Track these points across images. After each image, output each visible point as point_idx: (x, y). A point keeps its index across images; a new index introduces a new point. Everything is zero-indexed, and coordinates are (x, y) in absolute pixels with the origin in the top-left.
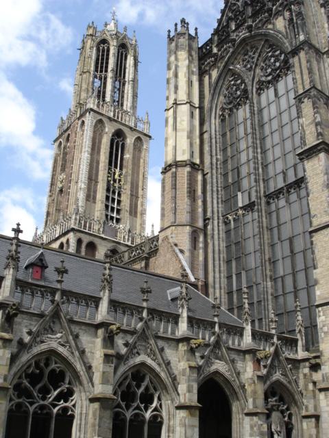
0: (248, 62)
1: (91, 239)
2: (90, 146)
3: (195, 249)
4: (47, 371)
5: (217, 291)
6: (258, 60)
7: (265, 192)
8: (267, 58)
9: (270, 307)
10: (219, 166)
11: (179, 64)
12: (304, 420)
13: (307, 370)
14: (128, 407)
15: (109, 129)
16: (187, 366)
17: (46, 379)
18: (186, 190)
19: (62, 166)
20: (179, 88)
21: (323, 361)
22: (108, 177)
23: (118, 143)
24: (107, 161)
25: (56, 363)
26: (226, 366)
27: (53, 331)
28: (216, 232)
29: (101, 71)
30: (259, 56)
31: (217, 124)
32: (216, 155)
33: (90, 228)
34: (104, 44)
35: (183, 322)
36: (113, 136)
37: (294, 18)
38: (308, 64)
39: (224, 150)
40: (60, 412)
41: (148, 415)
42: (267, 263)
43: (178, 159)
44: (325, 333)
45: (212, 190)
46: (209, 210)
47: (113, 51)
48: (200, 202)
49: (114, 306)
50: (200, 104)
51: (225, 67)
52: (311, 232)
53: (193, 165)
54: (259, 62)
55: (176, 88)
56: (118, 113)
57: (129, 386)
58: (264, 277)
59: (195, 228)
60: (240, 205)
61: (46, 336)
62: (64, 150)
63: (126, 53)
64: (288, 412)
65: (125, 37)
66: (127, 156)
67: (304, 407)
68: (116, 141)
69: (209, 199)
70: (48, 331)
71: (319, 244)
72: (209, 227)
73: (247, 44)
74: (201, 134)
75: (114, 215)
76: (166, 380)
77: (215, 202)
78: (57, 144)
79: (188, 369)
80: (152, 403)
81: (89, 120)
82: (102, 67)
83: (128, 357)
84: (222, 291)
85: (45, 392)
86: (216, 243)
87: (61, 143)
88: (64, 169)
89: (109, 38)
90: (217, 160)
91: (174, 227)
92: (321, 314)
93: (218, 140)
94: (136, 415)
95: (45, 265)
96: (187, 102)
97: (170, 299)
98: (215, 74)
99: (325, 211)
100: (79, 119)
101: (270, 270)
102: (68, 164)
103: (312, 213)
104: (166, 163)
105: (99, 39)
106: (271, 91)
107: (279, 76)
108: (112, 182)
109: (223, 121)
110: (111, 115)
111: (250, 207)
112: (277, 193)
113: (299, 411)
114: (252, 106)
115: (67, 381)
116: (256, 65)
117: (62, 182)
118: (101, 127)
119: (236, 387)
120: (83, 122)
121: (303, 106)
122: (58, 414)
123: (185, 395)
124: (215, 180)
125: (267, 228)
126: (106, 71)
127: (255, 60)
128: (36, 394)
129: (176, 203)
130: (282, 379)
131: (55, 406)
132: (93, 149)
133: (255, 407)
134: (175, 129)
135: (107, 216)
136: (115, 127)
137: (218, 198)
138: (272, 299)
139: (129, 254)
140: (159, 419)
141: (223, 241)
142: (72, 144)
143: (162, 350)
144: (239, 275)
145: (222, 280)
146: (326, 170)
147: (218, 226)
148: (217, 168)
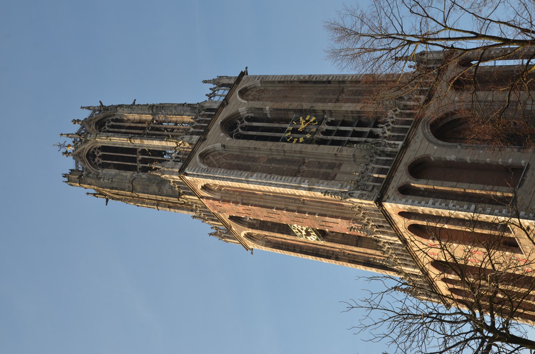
2: (239, 173)
22: (298, 142)
23: (243, 128)
24: (270, 144)
29: (134, 160)
34: (95, 156)
36: (231, 137)
47: (103, 140)
63: (113, 120)
65: (85, 123)
68: (240, 131)
89: (87, 147)
108: (308, 136)
118: (213, 156)
126: (133, 151)
132: (246, 169)
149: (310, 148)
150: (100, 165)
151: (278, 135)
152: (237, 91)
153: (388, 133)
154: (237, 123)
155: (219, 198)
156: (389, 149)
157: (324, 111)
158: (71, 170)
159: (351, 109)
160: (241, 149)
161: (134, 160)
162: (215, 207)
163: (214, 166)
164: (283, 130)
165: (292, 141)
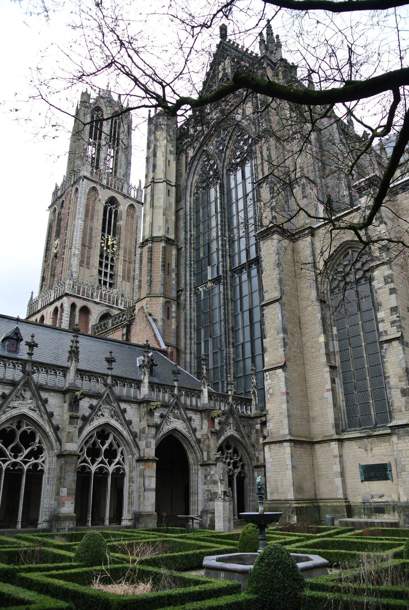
0: (221, 144)
1: (85, 303)
2: (84, 213)
3: (168, 318)
4: (19, 433)
5: (188, 356)
6: (228, 143)
7: (230, 267)
8: (238, 141)
9: (232, 370)
10: (192, 242)
11: (158, 144)
12: (255, 469)
13: (258, 427)
14: (93, 462)
15: (104, 195)
16: (146, 425)
17: (18, 440)
18: (160, 264)
19: (56, 232)
20: (157, 167)
21: (268, 419)
22: (102, 243)
24: (101, 228)
25: (27, 426)
26: (184, 424)
27: (24, 398)
28: (188, 303)
30: (230, 139)
31: (192, 201)
32: (190, 231)
33: (84, 292)
35: (144, 387)
36: (106, 203)
37: (259, 106)
38: (268, 152)
39: (197, 226)
40: (31, 467)
41: (111, 469)
42: (231, 332)
43: (155, 235)
44: (271, 394)
45: (186, 264)
46: (183, 282)
48: (173, 275)
49: (80, 375)
50: (176, 182)
51: (199, 148)
52: (263, 306)
53: (168, 241)
54: (230, 145)
55: (154, 167)
56: (112, 180)
57: (94, 443)
58: (227, 344)
59: (168, 300)
60: (209, 278)
61: (18, 402)
62: (58, 217)
64: (241, 463)
66: (121, 223)
67: (255, 459)
68: (109, 208)
69: (182, 273)
70: (19, 398)
71: (269, 317)
72: (182, 298)
73: (220, 127)
74: (177, 211)
75: (108, 280)
76: (128, 437)
77: (188, 275)
78: (52, 210)
79: (147, 429)
80: (115, 457)
81: (84, 186)
82: (96, 135)
83: (93, 419)
84: (193, 356)
85: (16, 451)
86: (188, 312)
87: (55, 210)
88: (59, 235)
90: (191, 236)
91: (149, 298)
92: (268, 378)
93: (192, 217)
94: (101, 469)
95: (20, 338)
96: (164, 181)
97: (138, 366)
98: (191, 153)
99: (275, 288)
100: (72, 186)
101: (233, 338)
102: (62, 231)
103: (265, 289)
104: (144, 237)
105: (93, 106)
106: (239, 174)
107: (246, 159)
108: (105, 248)
109: (197, 199)
110: (104, 182)
111: (217, 280)
112: (242, 267)
113: (251, 461)
114: (222, 186)
115: (37, 441)
116: (227, 148)
117: (56, 248)
118: (94, 194)
119: (192, 442)
120: (77, 189)
121: (262, 190)
122: (28, 470)
123: (144, 450)
124: (188, 254)
125: (231, 299)
126: (100, 139)
127: (226, 142)
128: (8, 453)
129: (151, 276)
130: (236, 434)
131: (25, 463)
132: (86, 216)
133: (209, 459)
134: (152, 206)
135: (100, 281)
136: (111, 194)
137: (190, 271)
138: (233, 363)
139: (113, 321)
140: (122, 471)
141: (194, 311)
142: (66, 211)
143: (124, 411)
144: (206, 342)
145: (193, 346)
146: (278, 250)
147: (190, 297)
148: (190, 243)
149: (98, 252)
150: (93, 115)
151: (106, 230)
152: (133, 203)
153: (104, 293)
154: (114, 205)
155: (72, 198)
156: (95, 294)
157: (118, 255)
158: (90, 95)
159: (119, 270)
160: (98, 211)
161: (95, 139)
162: (68, 194)
163: (88, 194)
164: (109, 233)
165: (102, 239)
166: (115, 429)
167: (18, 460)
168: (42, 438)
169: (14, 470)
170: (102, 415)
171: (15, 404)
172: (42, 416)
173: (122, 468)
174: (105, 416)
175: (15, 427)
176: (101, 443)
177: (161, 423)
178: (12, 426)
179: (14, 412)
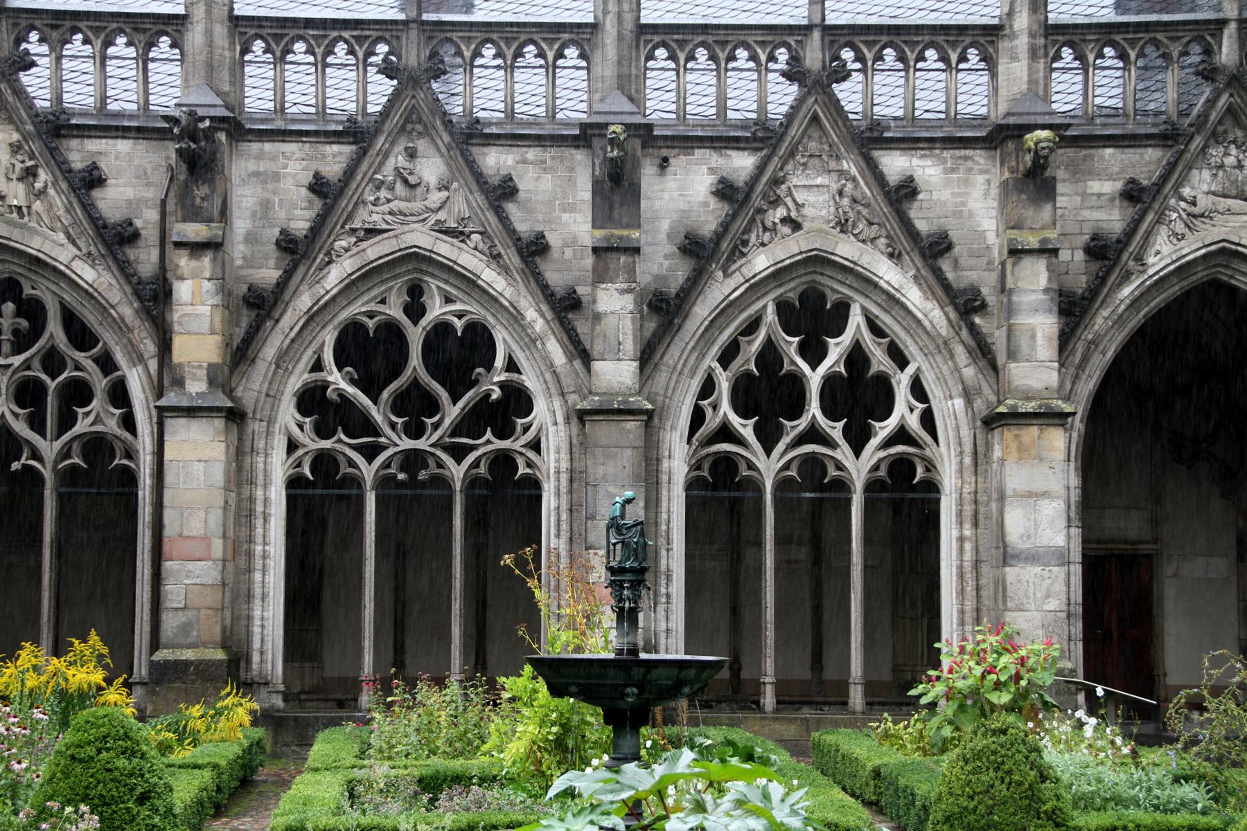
4: (416, 336)
14: (768, 438)
25: (448, 300)
35: (1014, 58)
57: (769, 353)
70: (391, 188)
83: (745, 243)
94: (813, 465)
122: (472, 483)
128: (378, 417)
140: (920, 473)
143: (906, 191)
166: (868, 283)
167: (422, 444)
168: (515, 347)
169: (413, 482)
170: (787, 220)
171: (375, 217)
172: (495, 257)
173: (924, 459)
174: (806, 225)
175: (395, 310)
176: (803, 350)
177: (1130, 233)
178: (381, 308)
179: (376, 250)
